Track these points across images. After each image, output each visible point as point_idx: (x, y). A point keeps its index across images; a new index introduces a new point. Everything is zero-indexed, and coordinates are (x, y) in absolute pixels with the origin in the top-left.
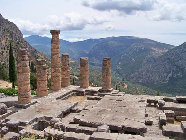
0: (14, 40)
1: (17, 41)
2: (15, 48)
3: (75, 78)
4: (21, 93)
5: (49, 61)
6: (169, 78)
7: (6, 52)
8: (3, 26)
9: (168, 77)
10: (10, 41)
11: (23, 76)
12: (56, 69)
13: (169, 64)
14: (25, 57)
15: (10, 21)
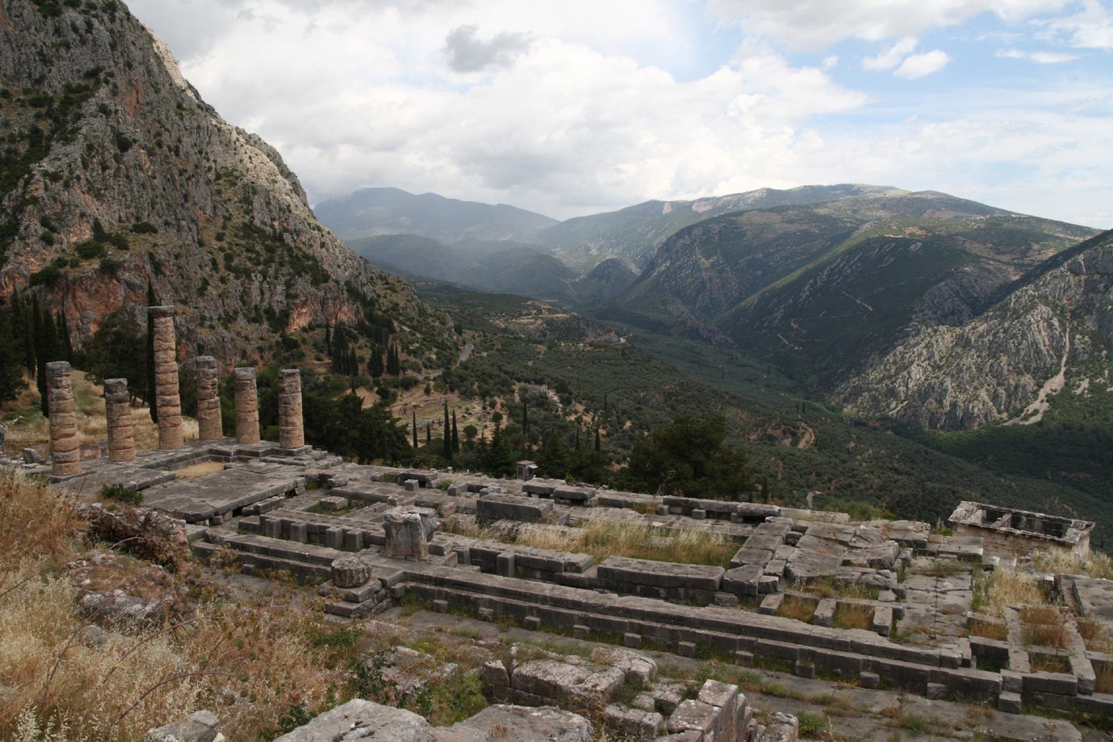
0: (257, 223)
1: (272, 226)
2: (262, 259)
3: (544, 397)
4: (56, 454)
5: (430, 320)
6: (1049, 398)
7: (223, 280)
8: (212, 158)
9: (1042, 394)
10: (237, 228)
11: (58, 421)
12: (164, 400)
13: (1051, 326)
14: (61, 381)
15: (249, 133)
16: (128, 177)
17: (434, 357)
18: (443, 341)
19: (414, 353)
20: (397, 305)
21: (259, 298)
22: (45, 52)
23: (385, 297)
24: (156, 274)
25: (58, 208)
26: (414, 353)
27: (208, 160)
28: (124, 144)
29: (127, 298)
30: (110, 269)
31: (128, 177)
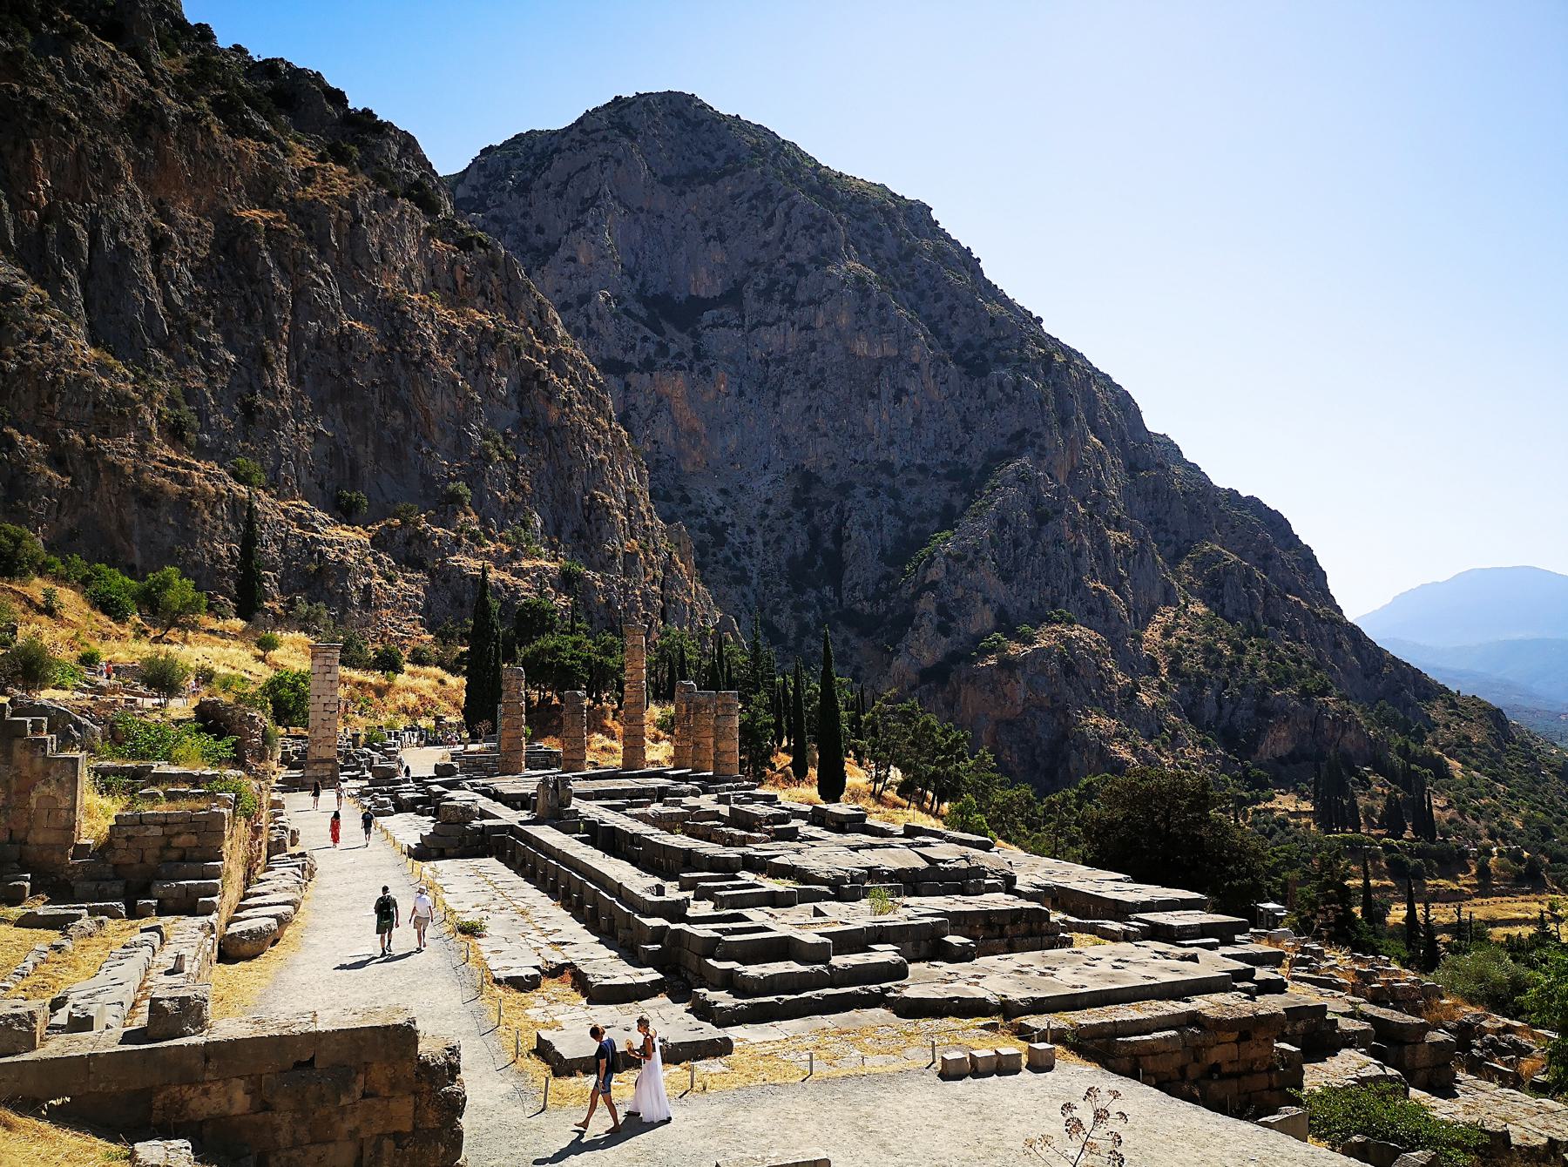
15: (1244, 494)
16: (1044, 554)
17: (1518, 824)
18: (1551, 801)
19: (1479, 813)
20: (1468, 738)
21: (1214, 712)
22: (968, 418)
23: (1447, 727)
24: (1067, 675)
25: (960, 592)
26: (1479, 813)
27: (1166, 531)
28: (1042, 519)
29: (1026, 700)
30: (1007, 664)
31: (1044, 554)
